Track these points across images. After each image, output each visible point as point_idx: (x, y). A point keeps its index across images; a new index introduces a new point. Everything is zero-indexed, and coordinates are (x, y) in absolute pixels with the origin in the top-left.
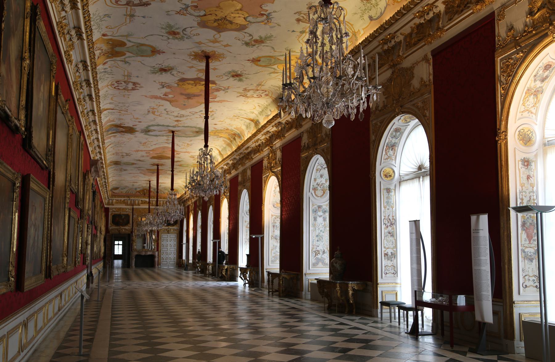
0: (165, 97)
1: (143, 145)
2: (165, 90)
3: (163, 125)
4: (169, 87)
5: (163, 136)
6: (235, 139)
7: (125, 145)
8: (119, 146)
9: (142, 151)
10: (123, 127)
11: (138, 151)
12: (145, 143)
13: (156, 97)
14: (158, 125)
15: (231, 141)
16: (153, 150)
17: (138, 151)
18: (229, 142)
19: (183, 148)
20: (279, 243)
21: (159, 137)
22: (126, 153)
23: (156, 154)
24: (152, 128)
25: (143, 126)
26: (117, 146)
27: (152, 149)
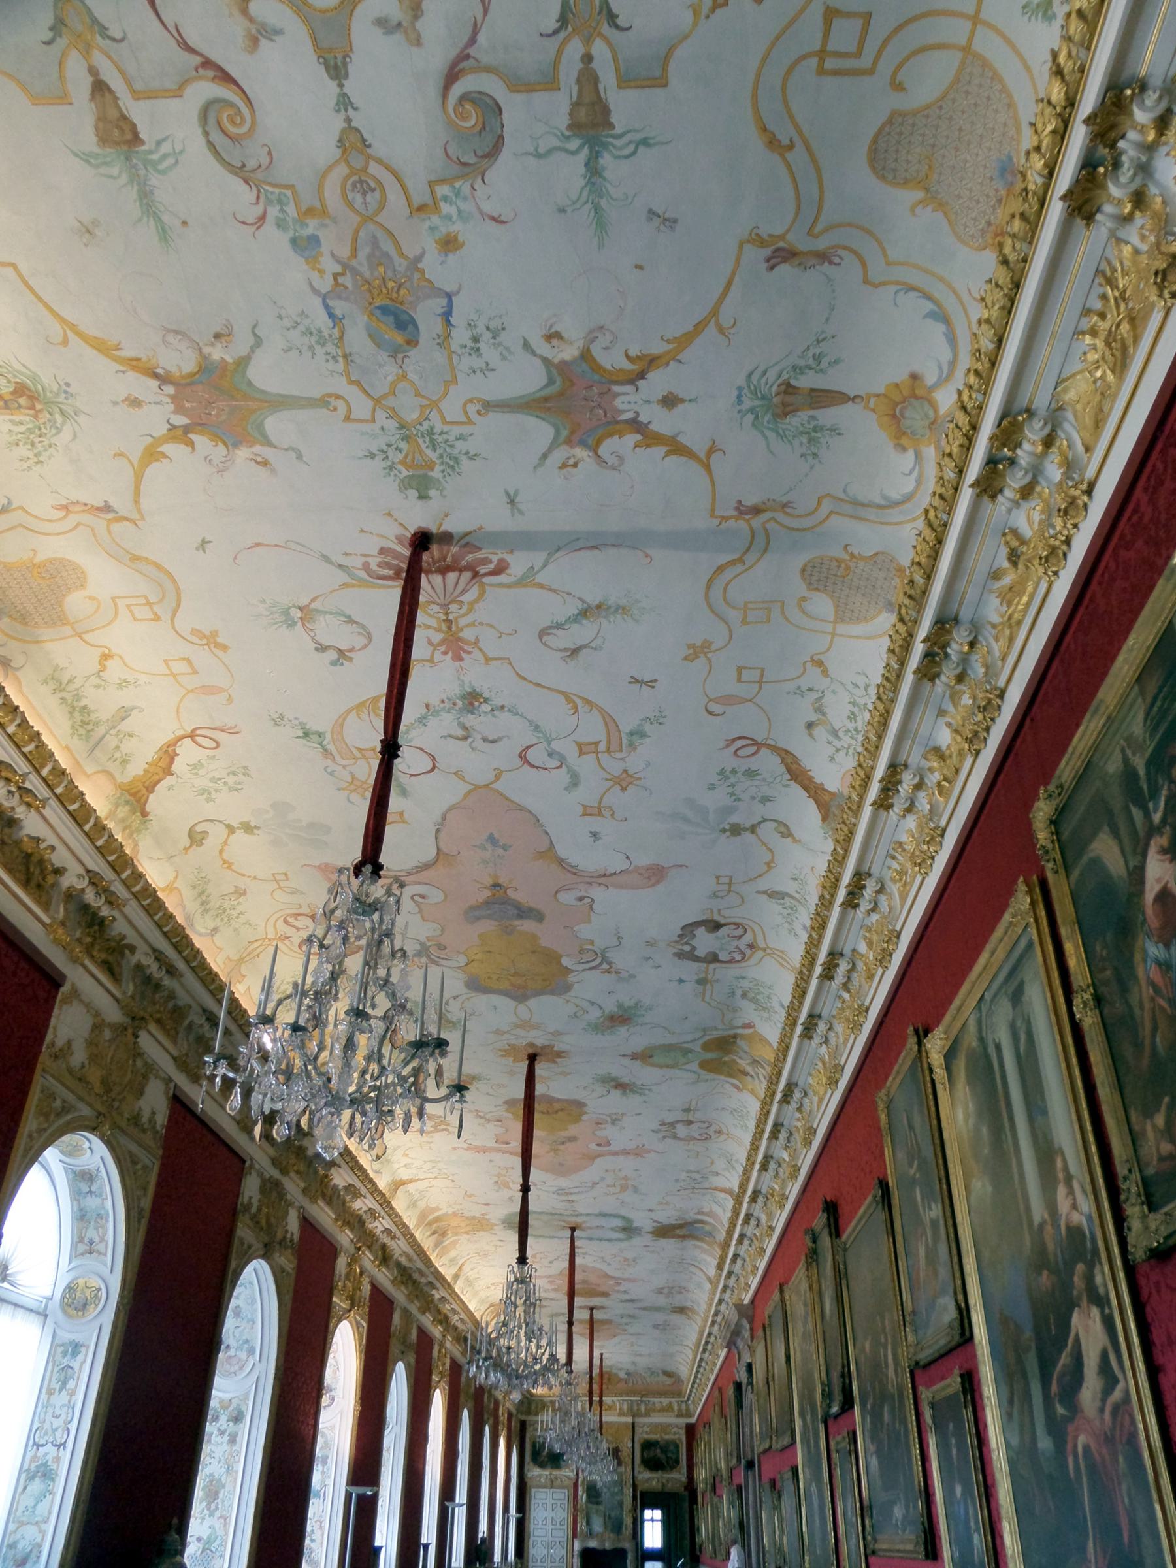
0: (618, 1281)
1: (626, 1178)
2: (622, 1288)
3: (601, 1240)
4: (618, 1291)
5: (588, 1215)
6: (434, 1233)
7: (677, 1180)
8: (694, 1175)
9: (626, 1153)
10: (679, 1236)
11: (639, 1152)
12: (624, 1188)
13: (629, 1280)
14: (609, 1240)
15: (430, 1224)
16: (592, 1158)
17: (639, 1152)
18: (430, 1217)
19: (507, 1169)
20: (310, 1515)
21: (597, 1211)
22: (675, 1137)
23: (572, 1139)
24: (621, 1236)
25: (637, 1241)
26: (698, 1176)
27: (597, 1161)
